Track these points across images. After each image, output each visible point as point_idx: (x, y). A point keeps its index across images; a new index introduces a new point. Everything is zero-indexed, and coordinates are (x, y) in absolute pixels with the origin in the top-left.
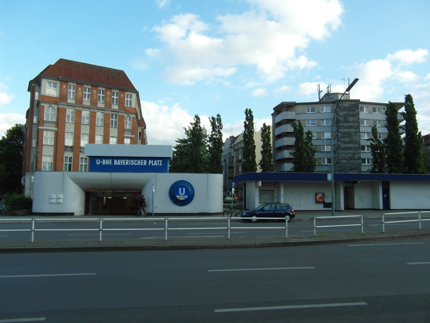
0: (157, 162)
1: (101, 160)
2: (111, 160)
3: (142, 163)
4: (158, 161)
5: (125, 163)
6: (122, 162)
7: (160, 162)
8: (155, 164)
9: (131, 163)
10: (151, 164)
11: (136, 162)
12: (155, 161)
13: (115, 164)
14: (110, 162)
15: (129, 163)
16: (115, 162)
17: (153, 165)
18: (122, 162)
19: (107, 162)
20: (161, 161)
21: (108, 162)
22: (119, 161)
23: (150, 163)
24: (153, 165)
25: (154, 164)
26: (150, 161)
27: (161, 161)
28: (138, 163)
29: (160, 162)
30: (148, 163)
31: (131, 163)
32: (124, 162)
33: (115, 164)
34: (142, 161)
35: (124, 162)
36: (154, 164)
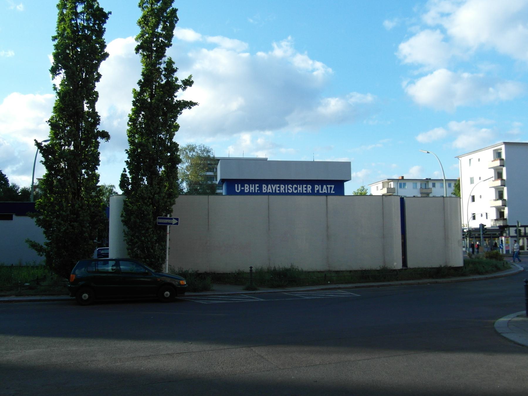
0: (327, 188)
1: (243, 186)
2: (257, 185)
3: (304, 189)
4: (329, 186)
5: (279, 190)
6: (274, 189)
7: (331, 188)
8: (324, 191)
9: (288, 189)
10: (318, 191)
11: (296, 189)
12: (325, 187)
13: (264, 191)
14: (257, 188)
15: (285, 189)
16: (264, 189)
17: (320, 192)
18: (274, 189)
19: (251, 188)
20: (333, 186)
21: (253, 188)
22: (269, 186)
23: (316, 189)
24: (320, 192)
25: (322, 190)
26: (316, 186)
27: (333, 186)
28: (299, 189)
29: (331, 188)
30: (313, 189)
31: (288, 189)
32: (277, 189)
33: (264, 191)
34: (304, 186)
35: (277, 189)
36: (322, 190)
